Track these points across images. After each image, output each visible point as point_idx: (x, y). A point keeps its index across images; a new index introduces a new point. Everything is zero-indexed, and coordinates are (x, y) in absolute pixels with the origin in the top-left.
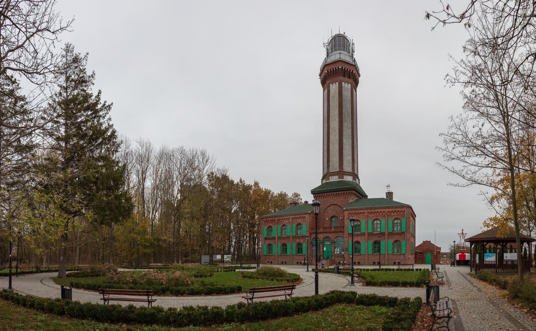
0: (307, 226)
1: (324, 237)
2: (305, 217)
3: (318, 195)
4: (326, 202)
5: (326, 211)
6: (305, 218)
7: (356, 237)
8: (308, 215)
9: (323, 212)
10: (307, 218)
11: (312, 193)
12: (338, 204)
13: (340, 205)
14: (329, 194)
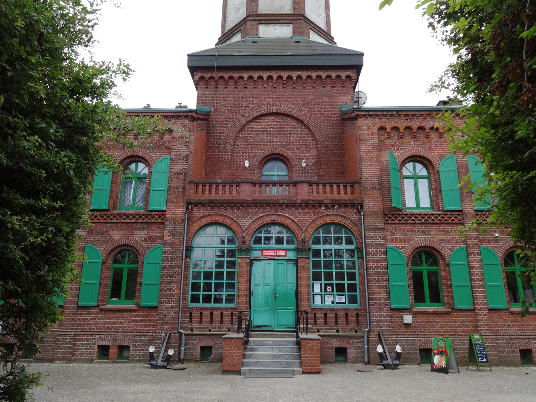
0: (178, 169)
1: (260, 223)
2: (170, 131)
3: (216, 75)
4: (245, 104)
5: (243, 134)
6: (167, 137)
7: (422, 228)
8: (186, 121)
9: (233, 136)
10: (177, 135)
11: (193, 69)
12: (294, 113)
13: (301, 115)
14: (260, 77)
